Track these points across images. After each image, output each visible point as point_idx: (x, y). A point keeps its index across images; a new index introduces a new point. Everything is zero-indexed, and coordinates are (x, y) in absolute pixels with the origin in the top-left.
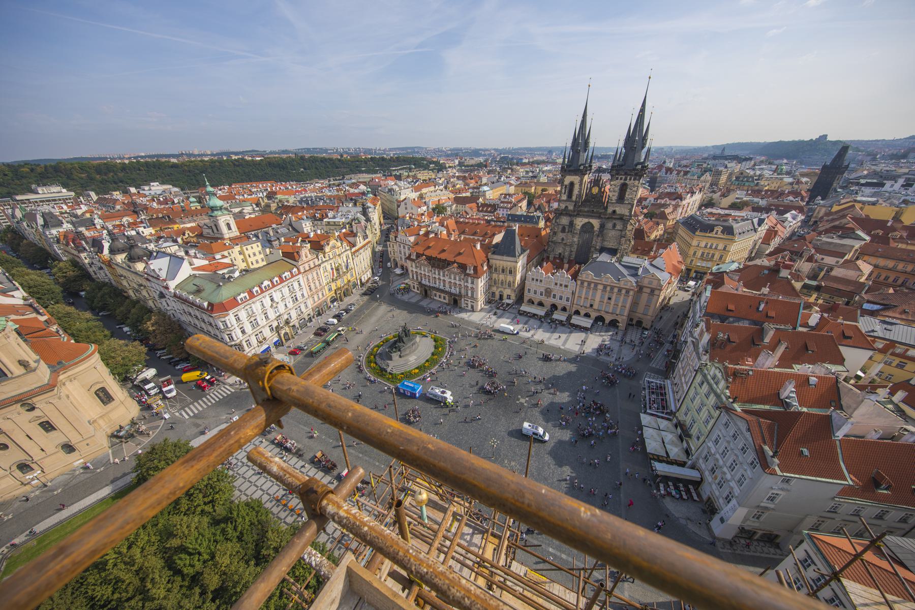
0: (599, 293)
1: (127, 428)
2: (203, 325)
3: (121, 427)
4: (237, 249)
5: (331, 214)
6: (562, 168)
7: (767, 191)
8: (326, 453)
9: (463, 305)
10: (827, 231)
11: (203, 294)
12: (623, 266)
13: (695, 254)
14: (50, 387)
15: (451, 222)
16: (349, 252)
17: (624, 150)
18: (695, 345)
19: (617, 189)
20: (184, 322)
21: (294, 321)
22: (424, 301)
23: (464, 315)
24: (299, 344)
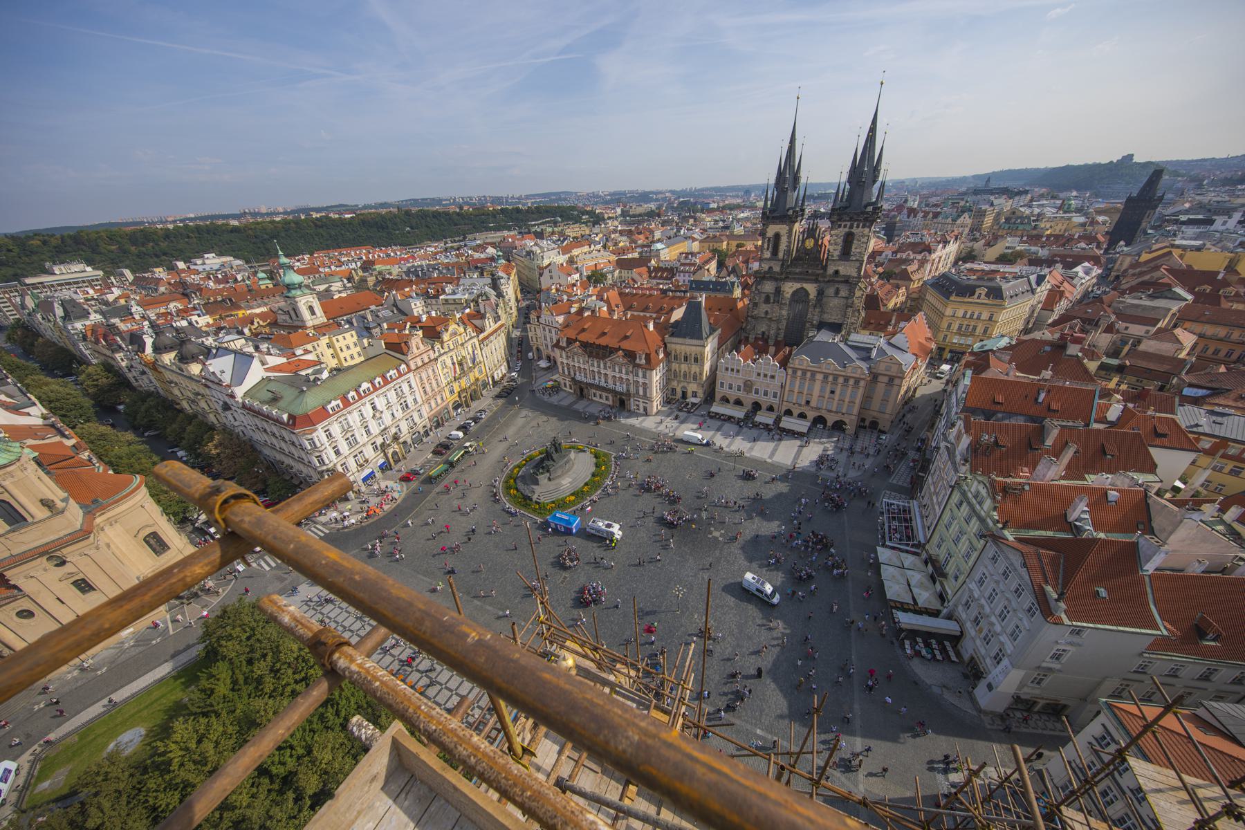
2: (283, 445)
4: (324, 340)
5: (449, 289)
6: (764, 214)
7: (1048, 236)
9: (633, 407)
10: (1132, 290)
11: (281, 404)
12: (850, 346)
13: (949, 326)
14: (83, 534)
15: (613, 295)
16: (475, 340)
17: (848, 186)
18: (951, 452)
19: (840, 241)
20: (258, 442)
21: (405, 436)
23: (634, 421)
24: (413, 467)
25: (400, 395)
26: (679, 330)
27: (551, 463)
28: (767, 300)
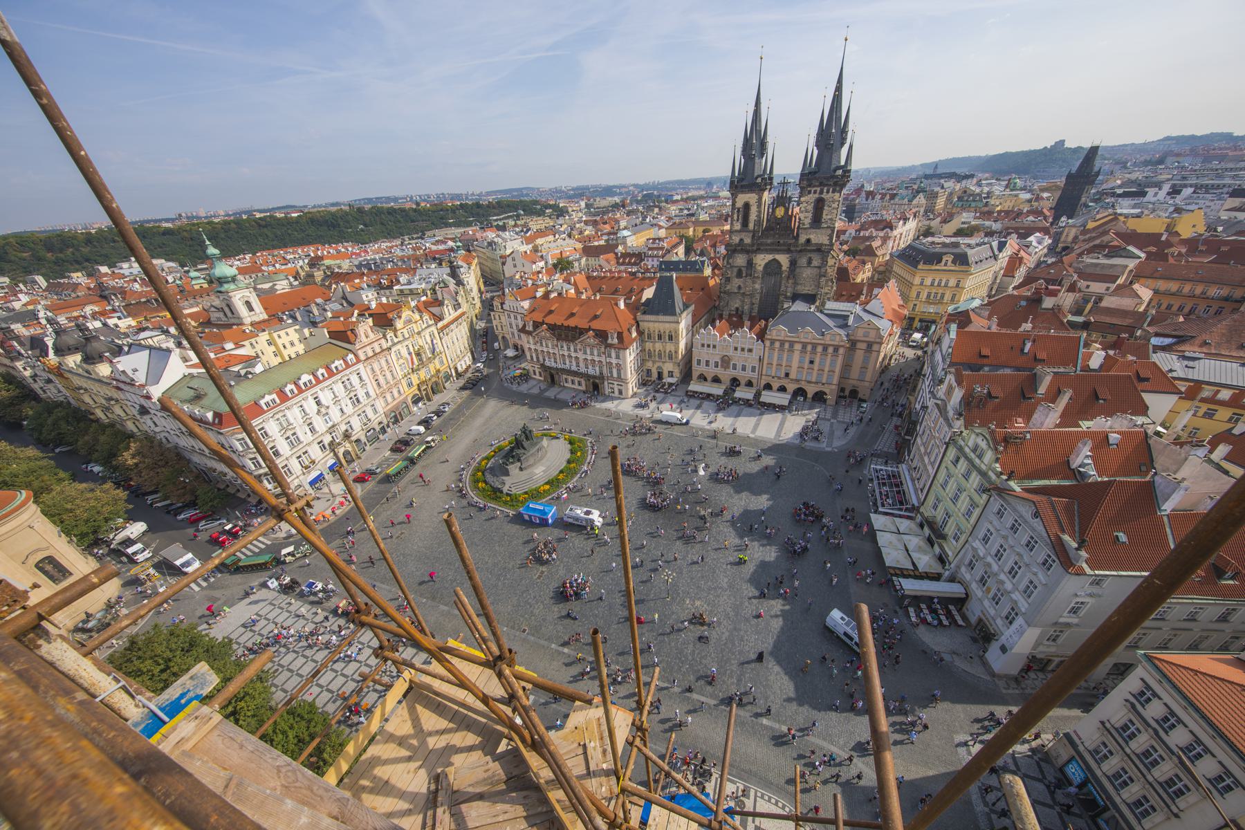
1: (99, 616)
3: (88, 615)
4: (264, 337)
5: (403, 279)
6: (732, 182)
7: (999, 212)
10: (1090, 251)
11: (205, 402)
12: (827, 315)
13: (919, 293)
16: (433, 328)
17: (816, 152)
18: (942, 409)
19: (810, 208)
20: (185, 448)
21: (358, 432)
22: (549, 391)
23: (609, 405)
24: (369, 466)
25: (348, 387)
26: (650, 308)
27: (521, 451)
28: (739, 275)
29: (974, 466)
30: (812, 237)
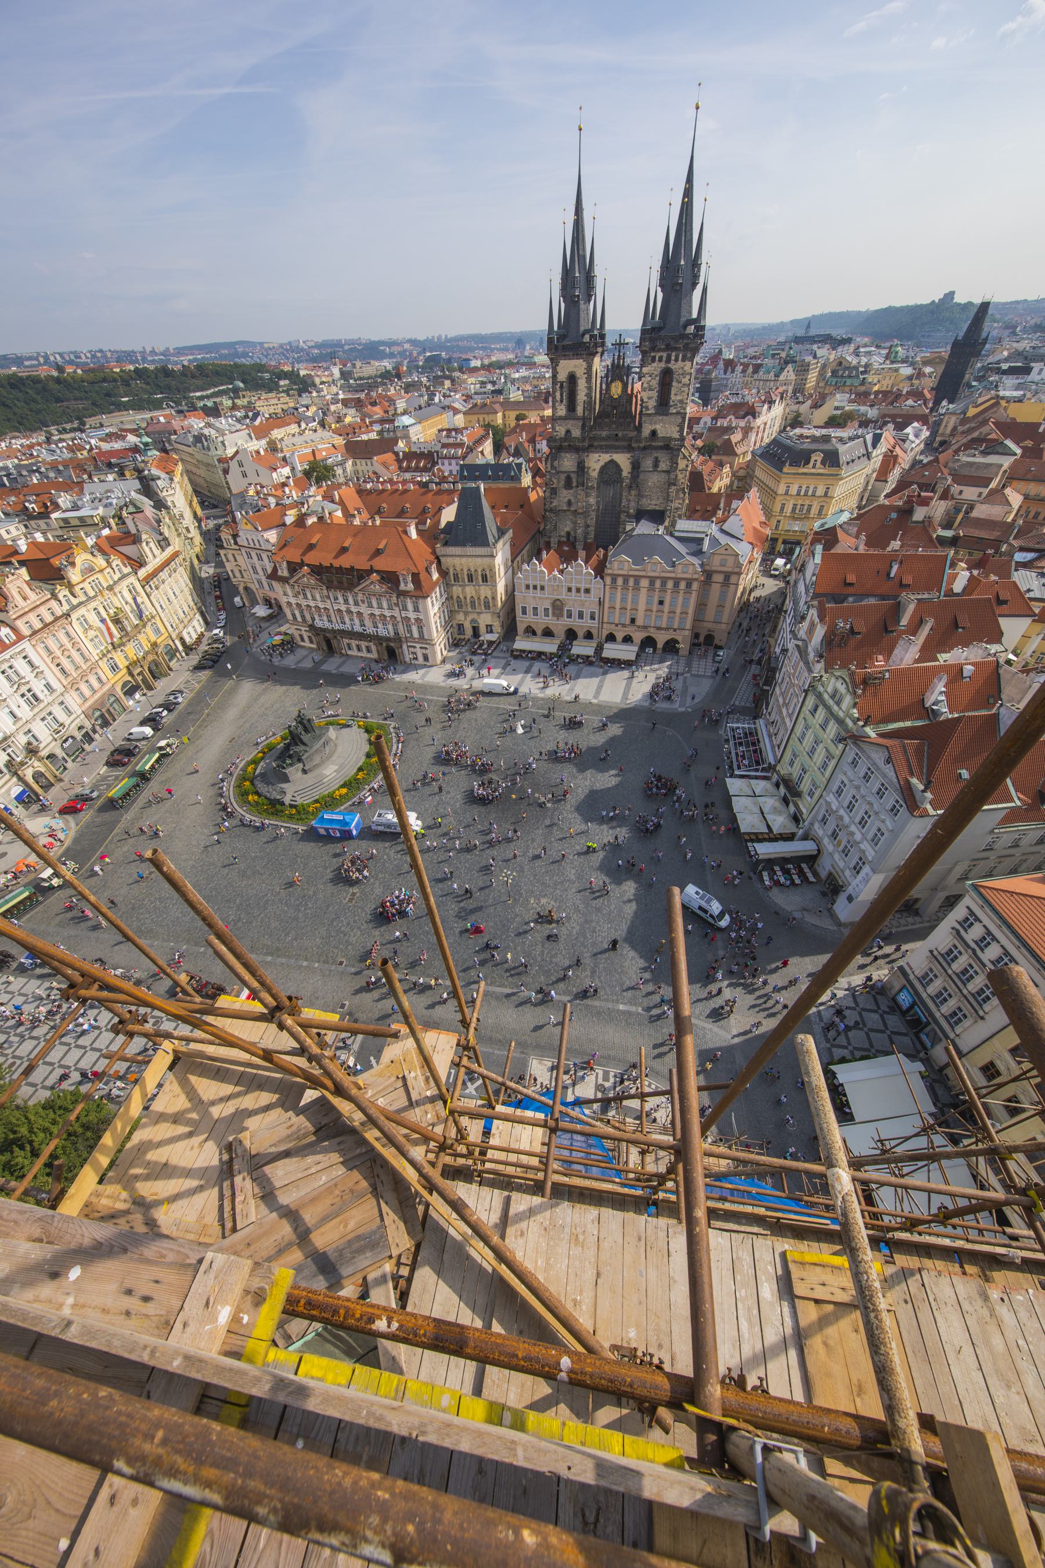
0: (643, 593)
5: (64, 500)
6: (550, 341)
7: (877, 393)
8: (193, 972)
9: (408, 657)
10: (968, 446)
13: (782, 509)
15: (348, 493)
16: (132, 579)
17: (660, 296)
18: (802, 651)
19: (655, 383)
22: (328, 660)
23: (412, 676)
24: (79, 790)
27: (300, 748)
28: (568, 485)
29: (832, 714)
30: (658, 427)
